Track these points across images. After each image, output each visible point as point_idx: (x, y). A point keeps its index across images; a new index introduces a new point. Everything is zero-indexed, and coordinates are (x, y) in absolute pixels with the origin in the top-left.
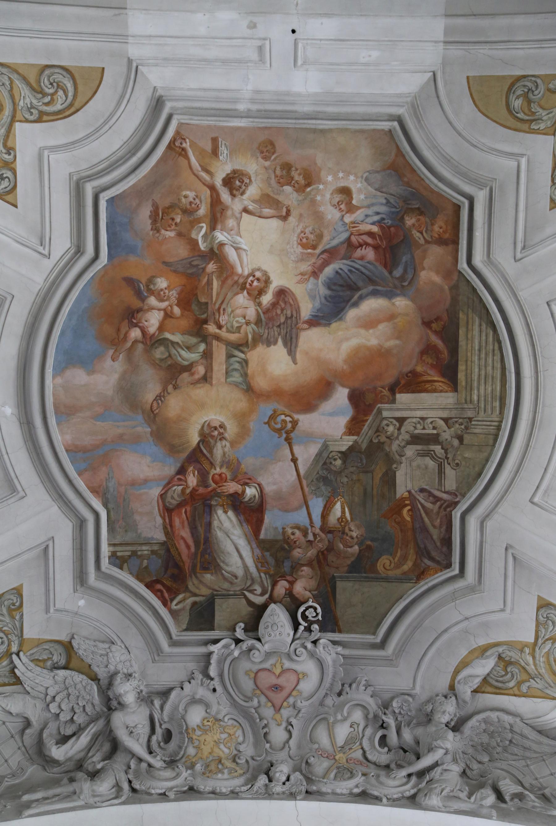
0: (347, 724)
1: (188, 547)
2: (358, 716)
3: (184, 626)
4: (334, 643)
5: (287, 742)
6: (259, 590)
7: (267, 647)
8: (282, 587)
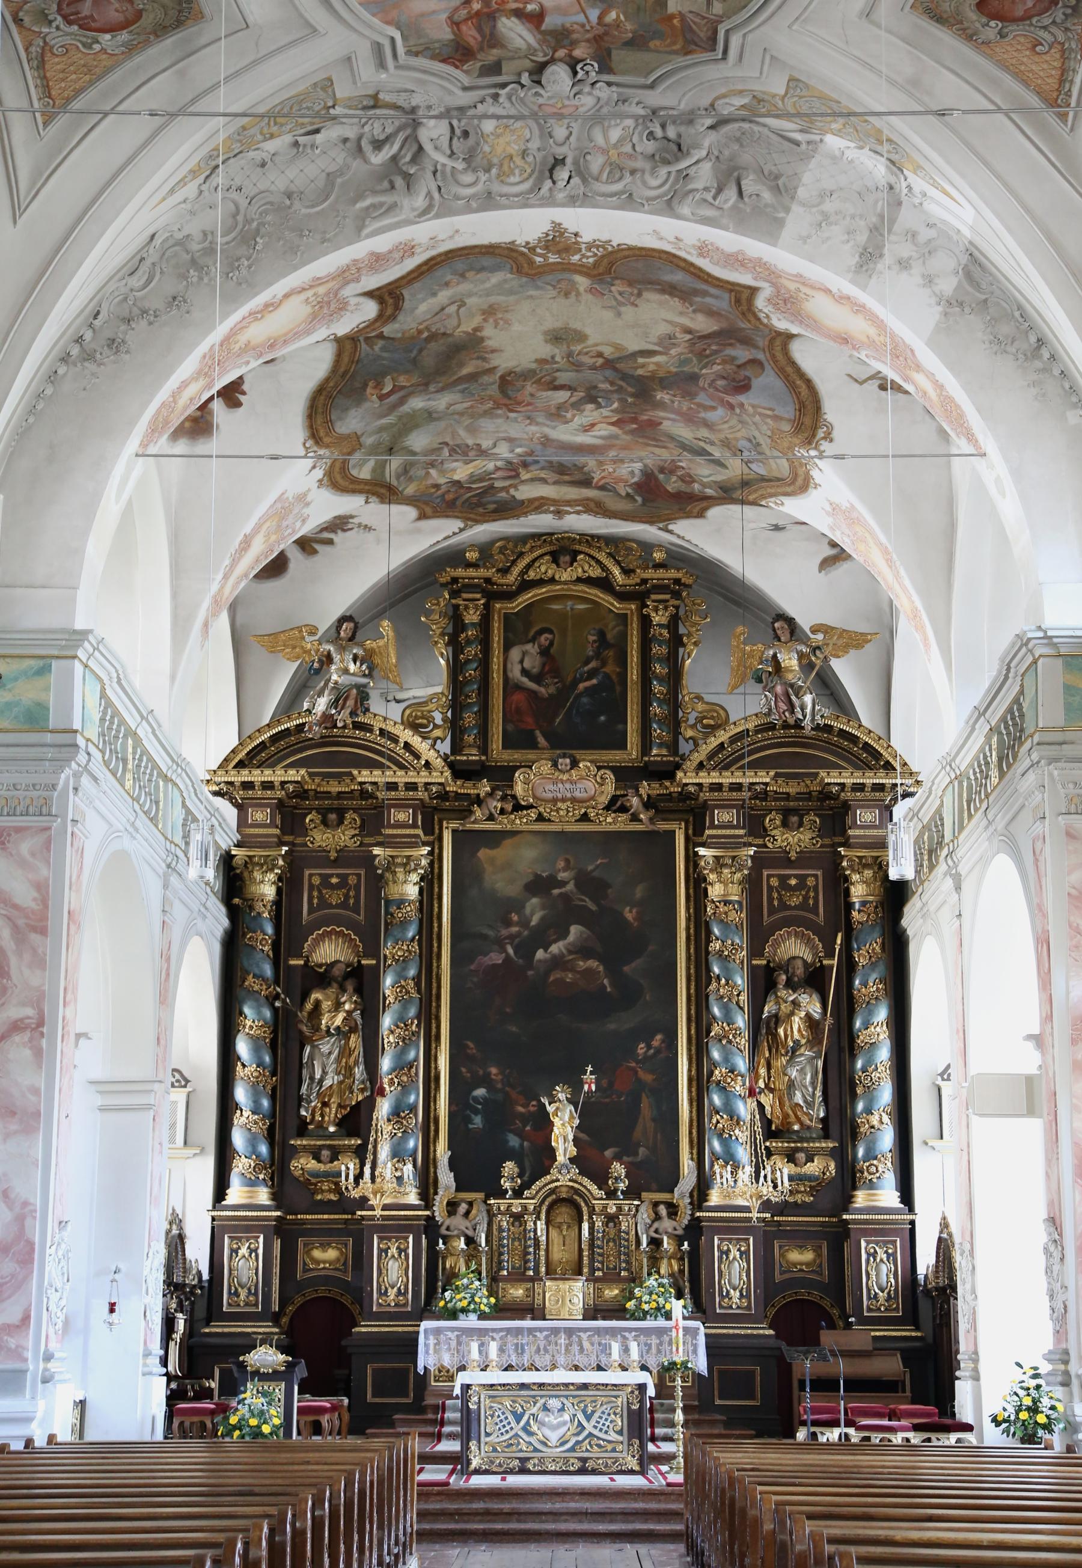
0: (620, 128)
1: (475, 38)
3: (476, 75)
4: (609, 84)
5: (568, 138)
6: (541, 54)
7: (549, 94)
8: (561, 53)
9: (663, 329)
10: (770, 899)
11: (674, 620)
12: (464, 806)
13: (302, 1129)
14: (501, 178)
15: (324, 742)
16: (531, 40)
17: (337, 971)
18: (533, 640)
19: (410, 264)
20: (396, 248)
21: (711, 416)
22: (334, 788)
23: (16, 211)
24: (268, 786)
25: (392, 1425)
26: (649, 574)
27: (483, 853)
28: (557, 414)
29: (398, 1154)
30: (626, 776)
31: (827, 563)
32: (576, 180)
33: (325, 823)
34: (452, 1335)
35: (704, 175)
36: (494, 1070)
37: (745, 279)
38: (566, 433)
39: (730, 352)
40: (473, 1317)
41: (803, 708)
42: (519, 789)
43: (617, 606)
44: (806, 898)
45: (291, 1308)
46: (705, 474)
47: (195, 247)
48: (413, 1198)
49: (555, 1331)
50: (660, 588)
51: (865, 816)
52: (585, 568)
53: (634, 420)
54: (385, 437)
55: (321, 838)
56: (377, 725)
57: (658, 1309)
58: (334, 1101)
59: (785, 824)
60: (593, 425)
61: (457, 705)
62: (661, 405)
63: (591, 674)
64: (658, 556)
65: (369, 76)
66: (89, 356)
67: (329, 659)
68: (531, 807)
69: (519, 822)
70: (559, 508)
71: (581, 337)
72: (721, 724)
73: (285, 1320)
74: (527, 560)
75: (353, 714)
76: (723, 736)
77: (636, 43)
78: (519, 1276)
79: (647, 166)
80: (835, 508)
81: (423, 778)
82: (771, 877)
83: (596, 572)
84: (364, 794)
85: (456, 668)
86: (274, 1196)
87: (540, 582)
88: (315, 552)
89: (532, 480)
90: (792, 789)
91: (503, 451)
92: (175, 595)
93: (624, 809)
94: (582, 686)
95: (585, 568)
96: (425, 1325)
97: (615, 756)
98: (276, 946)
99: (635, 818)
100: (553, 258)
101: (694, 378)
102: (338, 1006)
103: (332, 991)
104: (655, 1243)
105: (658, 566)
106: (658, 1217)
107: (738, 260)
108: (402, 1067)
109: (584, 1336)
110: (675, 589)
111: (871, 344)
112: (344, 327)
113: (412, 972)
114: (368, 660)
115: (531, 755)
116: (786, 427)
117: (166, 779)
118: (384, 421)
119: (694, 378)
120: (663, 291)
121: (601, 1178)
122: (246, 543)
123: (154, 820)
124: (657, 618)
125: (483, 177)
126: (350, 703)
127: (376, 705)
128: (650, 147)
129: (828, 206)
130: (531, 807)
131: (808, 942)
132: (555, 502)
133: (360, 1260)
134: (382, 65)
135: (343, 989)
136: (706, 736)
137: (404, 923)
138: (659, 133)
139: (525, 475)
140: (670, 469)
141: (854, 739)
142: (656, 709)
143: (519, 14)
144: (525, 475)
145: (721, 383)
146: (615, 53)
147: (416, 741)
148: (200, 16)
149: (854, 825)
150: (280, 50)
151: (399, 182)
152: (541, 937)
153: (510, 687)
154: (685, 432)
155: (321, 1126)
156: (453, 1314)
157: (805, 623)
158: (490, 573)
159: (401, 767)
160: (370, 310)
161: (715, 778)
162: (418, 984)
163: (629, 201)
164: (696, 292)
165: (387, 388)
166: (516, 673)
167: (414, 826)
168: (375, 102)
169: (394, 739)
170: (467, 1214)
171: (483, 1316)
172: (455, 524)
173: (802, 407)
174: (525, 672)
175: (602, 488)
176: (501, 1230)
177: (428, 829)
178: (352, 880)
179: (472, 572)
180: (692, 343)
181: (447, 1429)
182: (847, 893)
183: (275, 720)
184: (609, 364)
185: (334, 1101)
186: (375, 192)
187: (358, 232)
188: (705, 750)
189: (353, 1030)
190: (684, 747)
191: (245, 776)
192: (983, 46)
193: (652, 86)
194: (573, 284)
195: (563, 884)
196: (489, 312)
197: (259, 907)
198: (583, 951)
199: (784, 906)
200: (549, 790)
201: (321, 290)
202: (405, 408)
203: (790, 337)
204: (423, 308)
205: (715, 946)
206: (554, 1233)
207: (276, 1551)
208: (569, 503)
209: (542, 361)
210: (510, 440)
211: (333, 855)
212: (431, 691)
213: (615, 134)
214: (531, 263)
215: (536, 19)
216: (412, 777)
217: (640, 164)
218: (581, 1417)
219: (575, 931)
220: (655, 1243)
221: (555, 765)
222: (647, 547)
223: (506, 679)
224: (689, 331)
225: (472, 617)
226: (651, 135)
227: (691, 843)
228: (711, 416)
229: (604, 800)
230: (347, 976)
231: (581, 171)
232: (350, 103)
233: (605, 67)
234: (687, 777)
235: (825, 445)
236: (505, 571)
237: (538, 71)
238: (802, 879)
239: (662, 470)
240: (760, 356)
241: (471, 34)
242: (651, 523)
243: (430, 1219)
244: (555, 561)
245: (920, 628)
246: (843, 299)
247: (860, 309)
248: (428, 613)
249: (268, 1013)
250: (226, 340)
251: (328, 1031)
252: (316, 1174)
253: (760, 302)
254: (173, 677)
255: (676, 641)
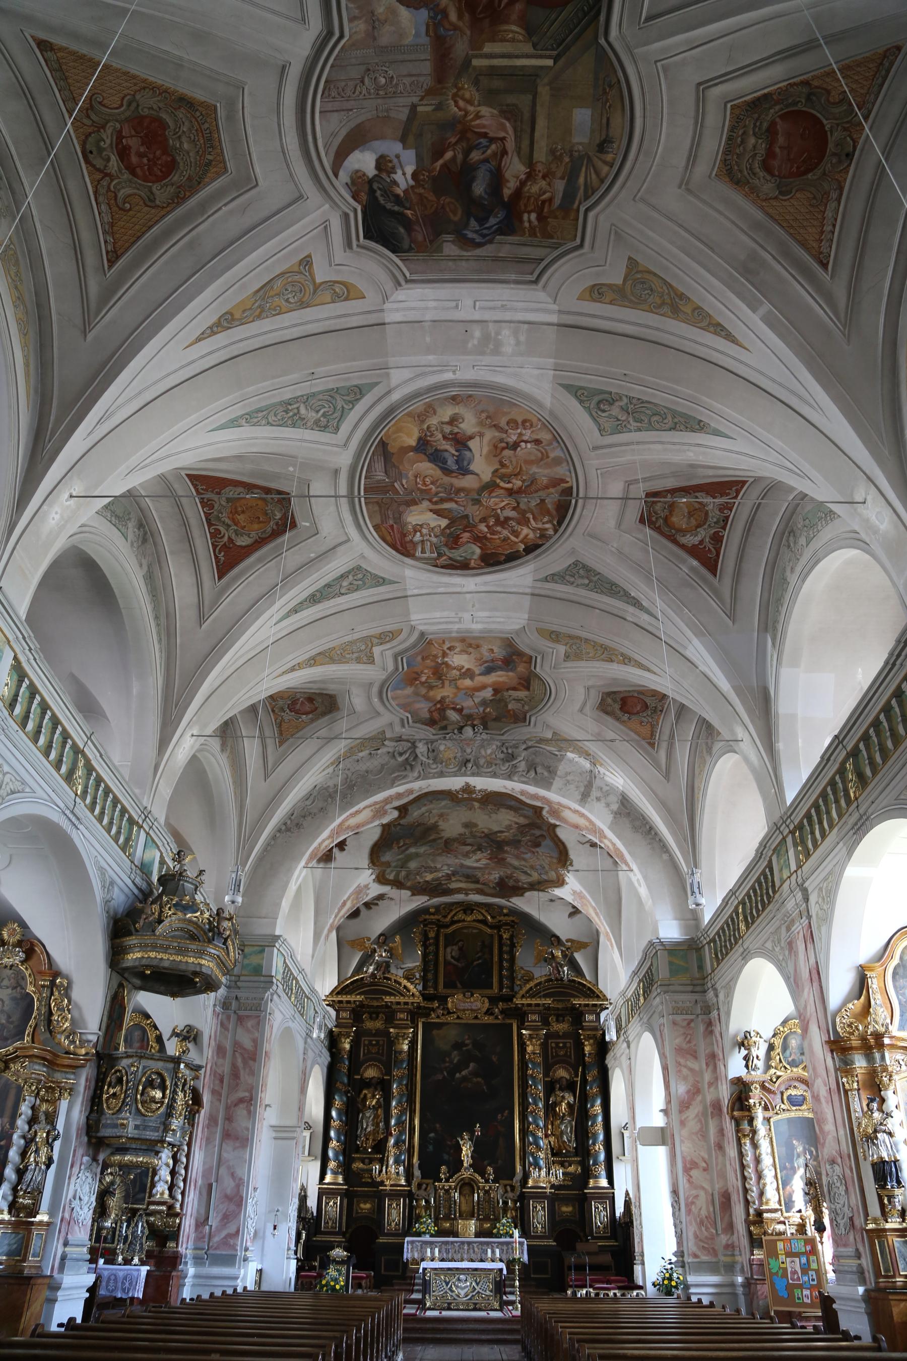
2: (494, 747)
8: (469, 723)
9: (507, 823)
10: (552, 1053)
11: (511, 938)
12: (426, 1012)
13: (357, 1150)
14: (446, 766)
15: (372, 984)
16: (458, 718)
17: (374, 1081)
18: (456, 944)
19: (411, 797)
20: (407, 791)
21: (526, 856)
22: (375, 1004)
23: (266, 777)
24: (348, 1002)
25: (392, 1285)
26: (502, 918)
27: (435, 1032)
28: (466, 855)
29: (397, 1162)
30: (493, 1000)
31: (571, 915)
32: (474, 767)
33: (371, 1018)
34: (419, 1244)
35: (522, 766)
36: (438, 1126)
37: (539, 804)
38: (469, 862)
39: (533, 832)
40: (428, 1236)
41: (564, 972)
42: (450, 1005)
43: (489, 931)
44: (566, 1052)
45: (350, 1230)
46: (523, 878)
47: (331, 790)
48: (403, 1182)
49: (463, 1243)
50: (506, 924)
51: (589, 1017)
52: (476, 916)
53: (496, 858)
54: (400, 863)
55: (369, 1025)
56: (393, 978)
57: (507, 1233)
58: (371, 1137)
59: (558, 1021)
60: (480, 859)
61: (425, 969)
62: (506, 852)
63: (479, 958)
64: (505, 911)
65: (398, 729)
66: (288, 830)
67: (374, 951)
68: (454, 1013)
69: (450, 1019)
70: (466, 892)
71: (476, 825)
72: (531, 979)
73: (348, 1235)
74: (453, 913)
75: (384, 973)
76: (532, 984)
77: (497, 719)
78: (447, 1218)
79: (501, 762)
80: (575, 892)
81: (411, 1000)
82: (552, 1043)
83: (481, 917)
84: (387, 1006)
85: (425, 955)
86: (344, 1179)
87: (459, 921)
88: (370, 908)
89: (456, 881)
90: (560, 1006)
91: (446, 870)
92: (315, 924)
93: (492, 1014)
94: (475, 963)
95: (476, 916)
96: (407, 1239)
97: (488, 992)
98: (349, 1070)
99: (497, 1018)
100: (465, 796)
101: (519, 841)
102: (374, 1096)
103: (372, 1090)
104: (505, 1203)
105: (505, 915)
106: (506, 1192)
107: (536, 797)
108: (400, 1123)
109: (475, 1245)
110: (512, 925)
111: (587, 828)
112: (385, 821)
113: (405, 1082)
114: (390, 951)
115: (454, 991)
116: (555, 861)
117: (308, 998)
118: (400, 857)
119: (519, 841)
120: (507, 808)
121: (483, 1174)
122: (344, 903)
123: (302, 1015)
124: (505, 936)
125: (440, 766)
126: (383, 969)
127: (393, 970)
128: (502, 756)
129: (569, 778)
130: (454, 1013)
131: (567, 1070)
132: (465, 889)
133: (380, 1209)
134: (403, 726)
135: (376, 1089)
136: (525, 984)
137: (402, 1061)
138: (505, 751)
139: (453, 879)
140: (510, 877)
141: (584, 985)
142: (505, 972)
143: (454, 709)
144: (453, 879)
145: (529, 843)
146: (489, 723)
147: (408, 984)
148: (338, 709)
149: (585, 1021)
150: (366, 721)
151: (408, 767)
152: (459, 1067)
153: (447, 963)
154: (516, 863)
155: (366, 1149)
156: (419, 1234)
157: (563, 938)
158: (439, 917)
159: (402, 995)
160: (396, 814)
161: (529, 1001)
162: (407, 1088)
163: (495, 775)
164: (520, 809)
165: (402, 844)
166: (449, 958)
167: (407, 1020)
168: (399, 739)
169: (400, 984)
170: (426, 1189)
171: (432, 1236)
172: (426, 898)
173: (561, 853)
174: (452, 957)
175: (484, 884)
176: (440, 1196)
177: (413, 1021)
178: (381, 1042)
179: (432, 917)
180: (518, 828)
181: (416, 1288)
182: (583, 1050)
183: (353, 976)
184: (487, 836)
185: (371, 1137)
186: (399, 771)
187: (392, 785)
188: (525, 989)
189: (380, 1107)
190: (516, 989)
191: (340, 998)
192: (623, 722)
193: (503, 735)
194: (473, 806)
195: (467, 1045)
196: (441, 816)
197: (343, 1053)
198: (475, 1074)
199: (557, 1055)
200: (462, 1006)
201: (378, 806)
202: (408, 852)
203: (556, 826)
204: (416, 814)
205: (530, 1072)
206: (462, 1198)
207: (338, 1356)
208: (471, 890)
209: (461, 835)
210: (447, 865)
211: (374, 1032)
212: (415, 964)
213: (489, 751)
214: (457, 797)
215: (460, 711)
216: (406, 1000)
217: (498, 762)
218: (474, 1284)
219: (472, 1065)
220: (505, 1203)
221: (464, 995)
222: (501, 908)
223: (445, 960)
224: (517, 823)
225: (432, 934)
226: (502, 752)
227: (519, 1029)
228: (526, 856)
229: (484, 1010)
230: (378, 1083)
231: (476, 764)
232: (391, 739)
233: (485, 728)
234: (518, 1001)
235: (570, 868)
236: (445, 917)
237: (460, 729)
238: (565, 1044)
239: (507, 877)
240: (544, 833)
241: (436, 716)
242: (503, 898)
243: (410, 1191)
244: (465, 913)
245: (609, 940)
246: (576, 812)
247: (582, 815)
248: (414, 933)
249: (345, 1099)
250: (340, 825)
251: (369, 1108)
252: (363, 1170)
253: (544, 813)
254: (313, 956)
255: (513, 946)
